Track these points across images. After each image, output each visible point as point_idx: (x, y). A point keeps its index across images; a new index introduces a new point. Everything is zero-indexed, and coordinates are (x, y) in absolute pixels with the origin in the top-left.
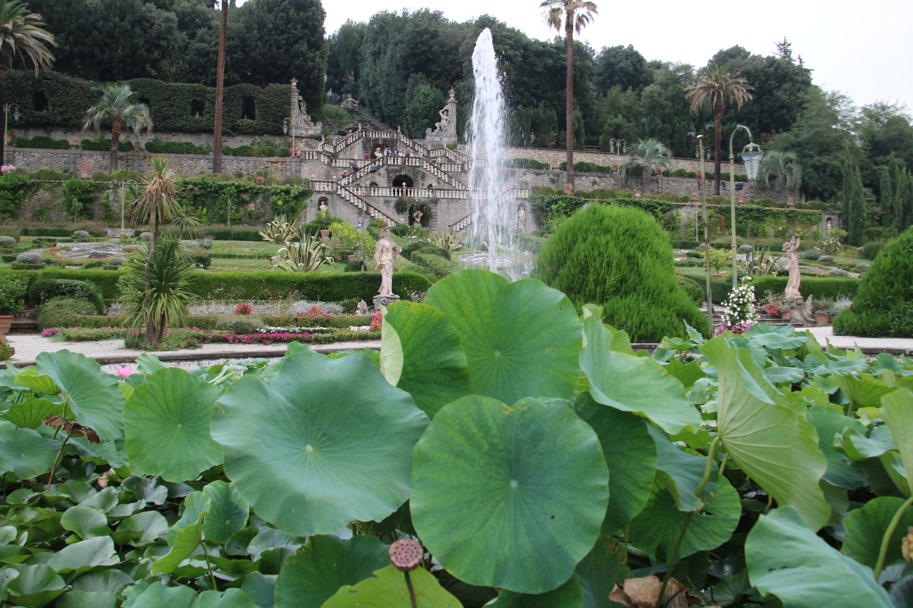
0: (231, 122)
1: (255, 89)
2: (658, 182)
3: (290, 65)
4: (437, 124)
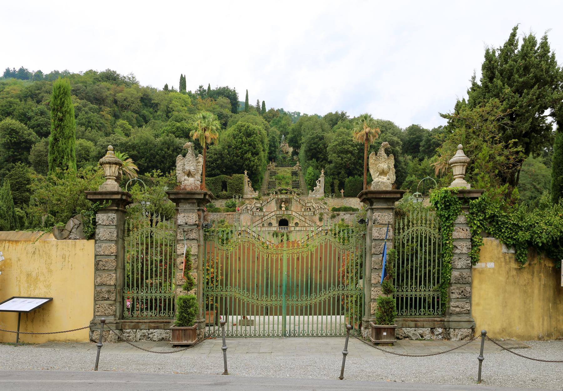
1: (226, 178)
3: (243, 164)
4: (314, 188)
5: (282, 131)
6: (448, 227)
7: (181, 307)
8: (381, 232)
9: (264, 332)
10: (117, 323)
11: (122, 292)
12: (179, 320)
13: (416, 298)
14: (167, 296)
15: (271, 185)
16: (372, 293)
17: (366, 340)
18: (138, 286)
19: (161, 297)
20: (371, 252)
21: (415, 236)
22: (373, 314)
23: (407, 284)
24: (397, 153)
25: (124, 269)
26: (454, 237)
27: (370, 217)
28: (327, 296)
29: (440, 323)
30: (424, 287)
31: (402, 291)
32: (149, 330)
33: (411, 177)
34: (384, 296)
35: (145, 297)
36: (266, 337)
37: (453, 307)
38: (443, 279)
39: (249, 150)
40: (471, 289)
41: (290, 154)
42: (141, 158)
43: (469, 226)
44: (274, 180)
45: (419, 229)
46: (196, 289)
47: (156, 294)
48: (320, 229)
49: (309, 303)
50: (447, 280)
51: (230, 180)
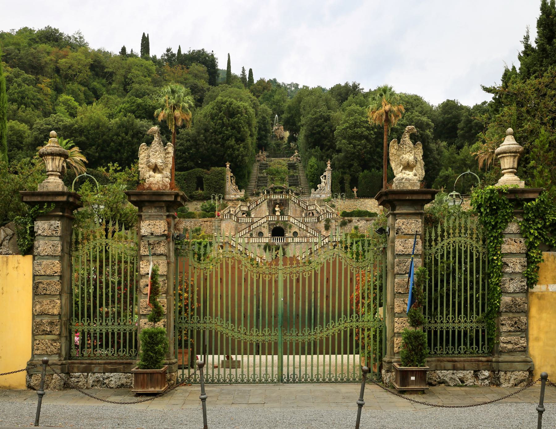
0: (190, 193)
4: (318, 186)
5: (275, 111)
6: (496, 238)
7: (146, 344)
8: (406, 245)
9: (254, 377)
10: (62, 364)
11: (68, 324)
12: (143, 361)
13: (454, 332)
14: (128, 330)
15: (261, 182)
16: (396, 325)
17: (390, 387)
18: (89, 316)
19: (119, 330)
20: (394, 271)
21: (451, 250)
22: (397, 353)
23: (442, 313)
24: (428, 138)
25: (71, 294)
26: (503, 252)
27: (392, 225)
28: (336, 329)
29: (486, 363)
30: (464, 317)
31: (436, 322)
32: (104, 373)
33: (447, 170)
34: (411, 329)
35: (98, 330)
36: (257, 383)
37: (503, 343)
38: (490, 307)
39: (232, 136)
40: (527, 320)
41: (286, 140)
42: (91, 145)
43: (524, 236)
44: (265, 174)
45: (457, 241)
46: (166, 320)
47: (113, 327)
48: (327, 240)
49: (312, 338)
50: (496, 307)
51: (207, 176)
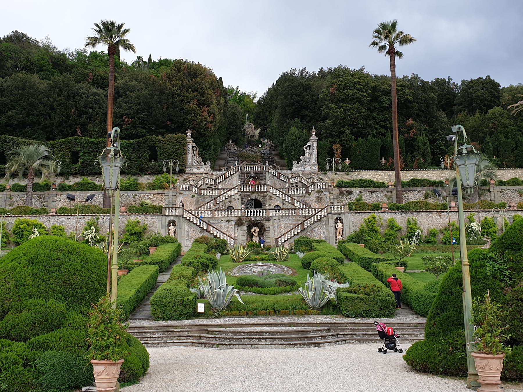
2: (489, 191)
4: (301, 157)
5: (245, 112)
41: (257, 137)
48: (323, 213)
